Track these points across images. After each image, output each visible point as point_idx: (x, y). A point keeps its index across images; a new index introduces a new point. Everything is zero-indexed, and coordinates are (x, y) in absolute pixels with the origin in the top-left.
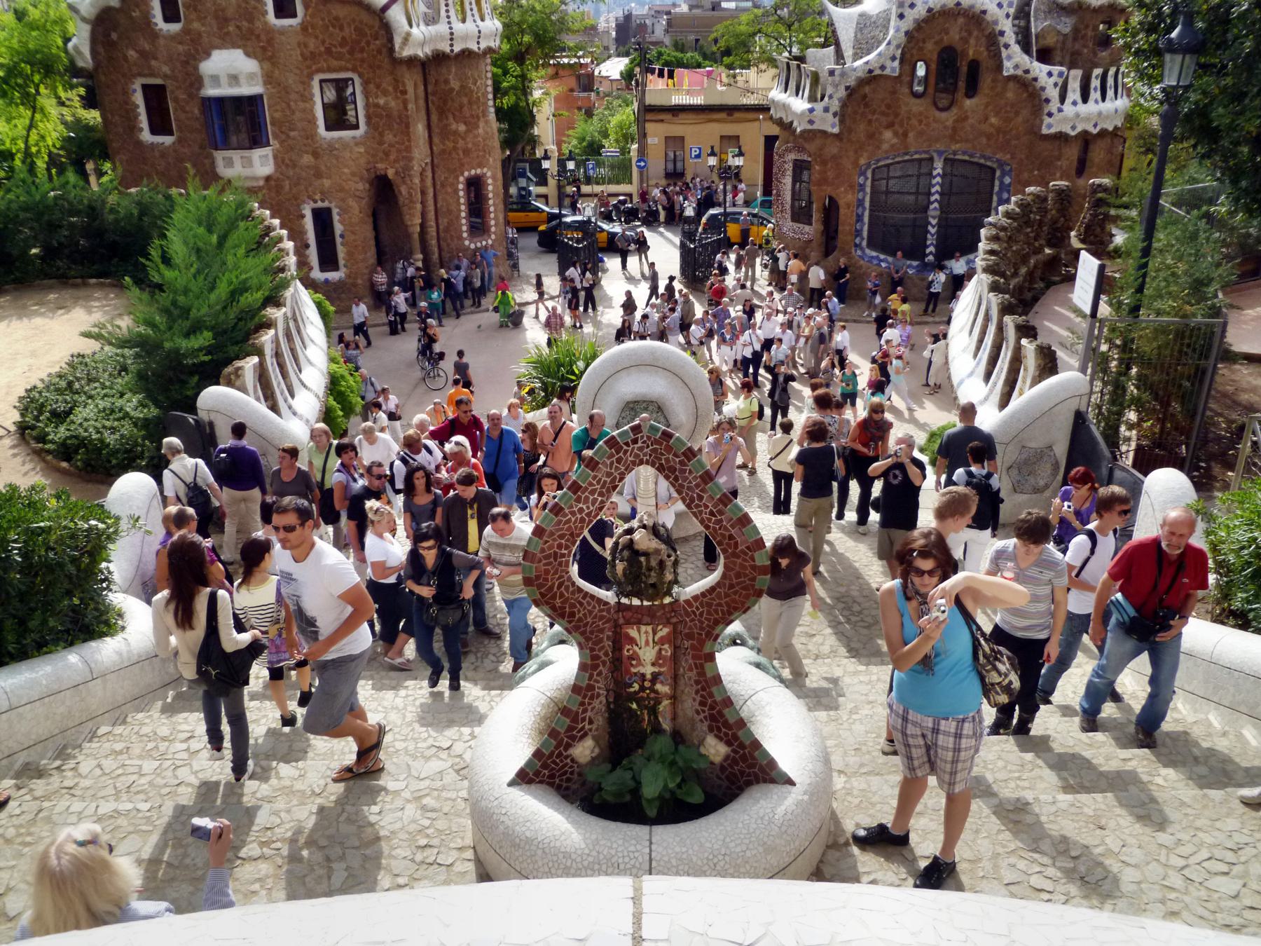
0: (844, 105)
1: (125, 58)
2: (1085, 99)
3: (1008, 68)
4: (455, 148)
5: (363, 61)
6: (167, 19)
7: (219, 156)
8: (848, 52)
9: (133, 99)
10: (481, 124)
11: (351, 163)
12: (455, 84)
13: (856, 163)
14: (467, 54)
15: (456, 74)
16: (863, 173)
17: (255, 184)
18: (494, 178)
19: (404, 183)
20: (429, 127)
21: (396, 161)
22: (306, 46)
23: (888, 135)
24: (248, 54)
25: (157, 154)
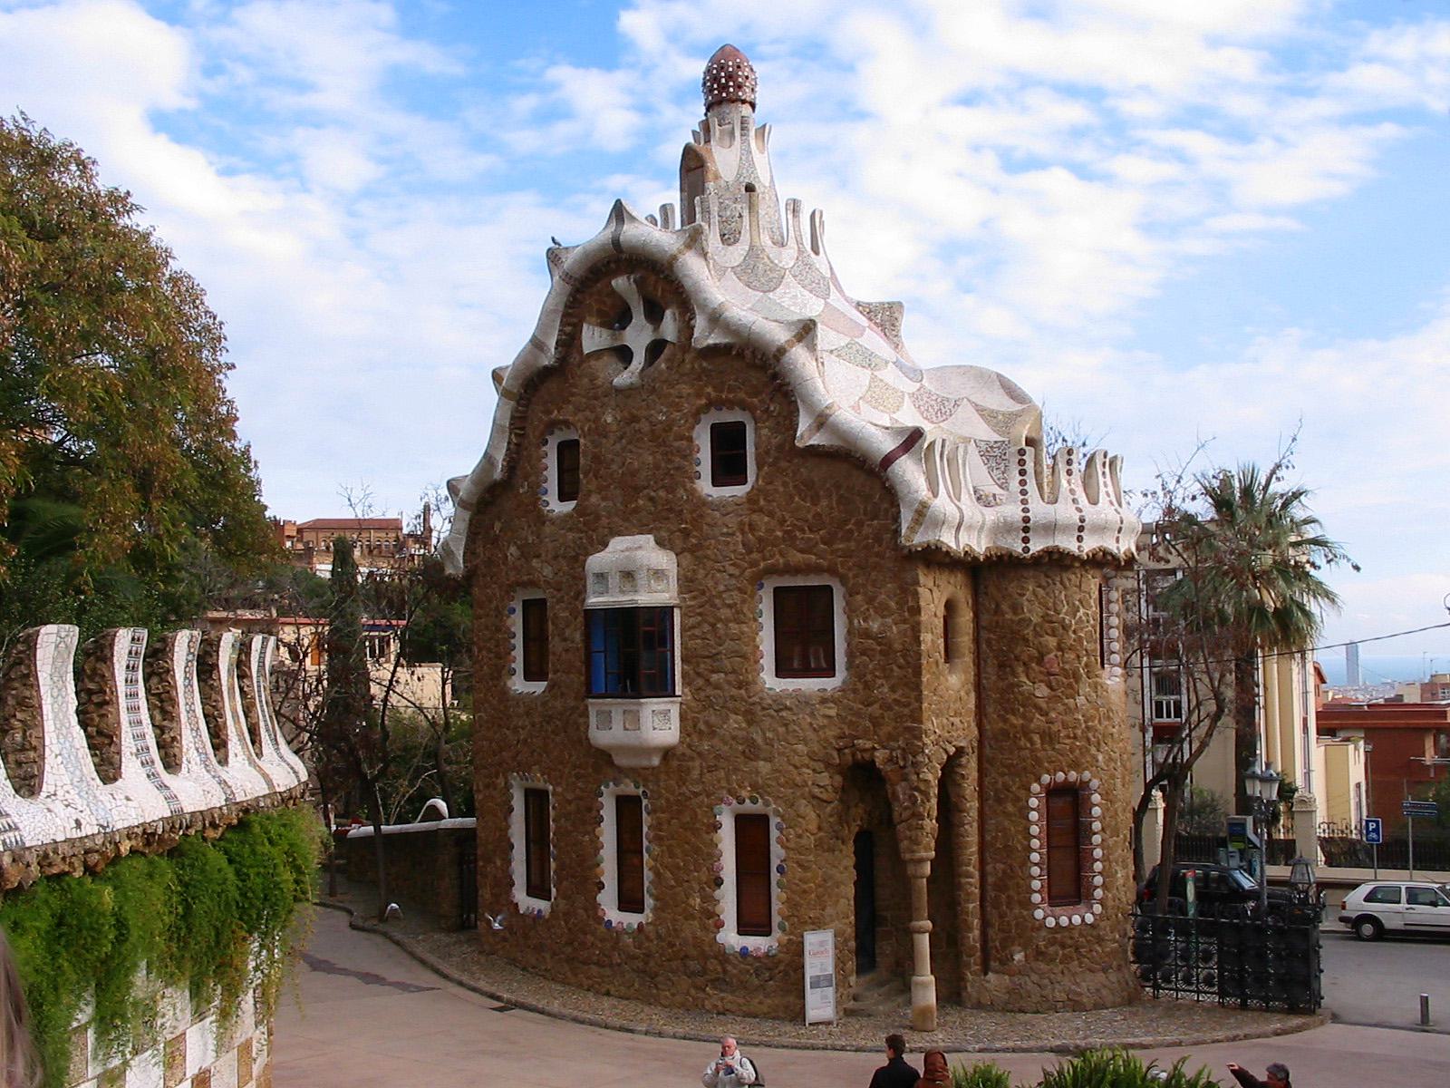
4: (1026, 733)
5: (848, 554)
6: (563, 497)
9: (509, 622)
10: (1085, 688)
11: (810, 734)
12: (1034, 614)
14: (1056, 561)
15: (1034, 593)
17: (645, 763)
18: (1107, 795)
19: (905, 778)
20: (979, 687)
21: (891, 737)
22: (752, 528)
24: (660, 543)
25: (521, 710)
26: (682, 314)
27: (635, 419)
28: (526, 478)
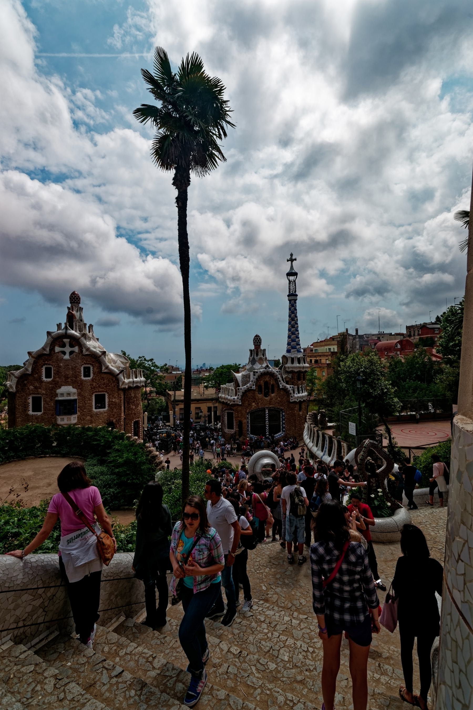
0: (242, 396)
1: (28, 389)
2: (299, 393)
3: (281, 387)
4: (132, 413)
5: (109, 389)
6: (46, 377)
7: (59, 418)
8: (241, 384)
12: (133, 395)
13: (246, 411)
16: (248, 414)
20: (124, 407)
22: (92, 385)
23: (254, 404)
24: (73, 387)
25: (34, 418)
26: (79, 348)
27: (68, 365)
28: (37, 373)
